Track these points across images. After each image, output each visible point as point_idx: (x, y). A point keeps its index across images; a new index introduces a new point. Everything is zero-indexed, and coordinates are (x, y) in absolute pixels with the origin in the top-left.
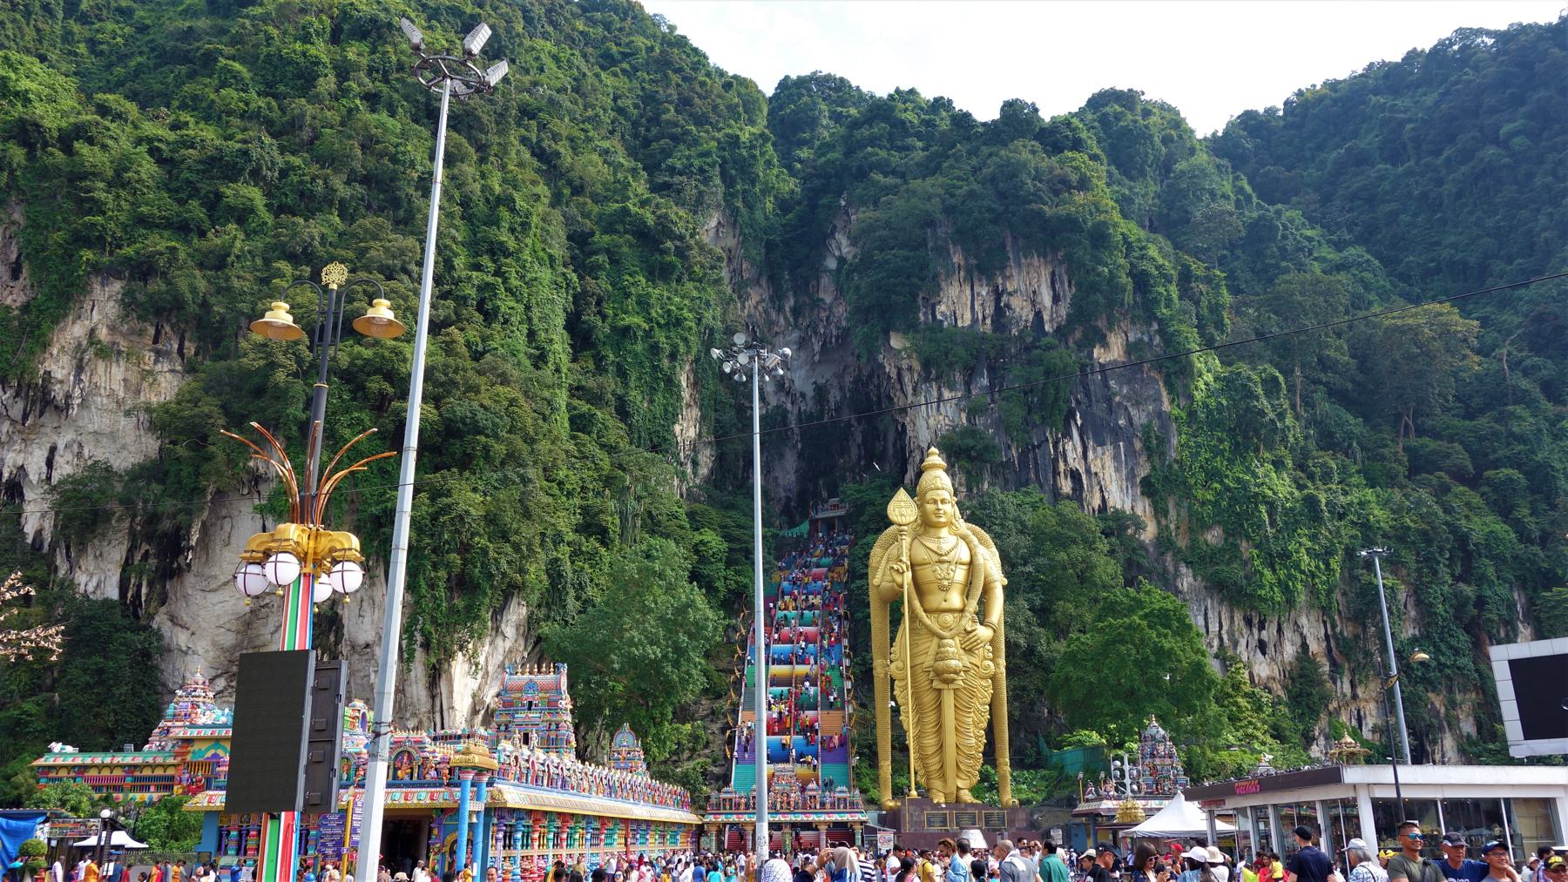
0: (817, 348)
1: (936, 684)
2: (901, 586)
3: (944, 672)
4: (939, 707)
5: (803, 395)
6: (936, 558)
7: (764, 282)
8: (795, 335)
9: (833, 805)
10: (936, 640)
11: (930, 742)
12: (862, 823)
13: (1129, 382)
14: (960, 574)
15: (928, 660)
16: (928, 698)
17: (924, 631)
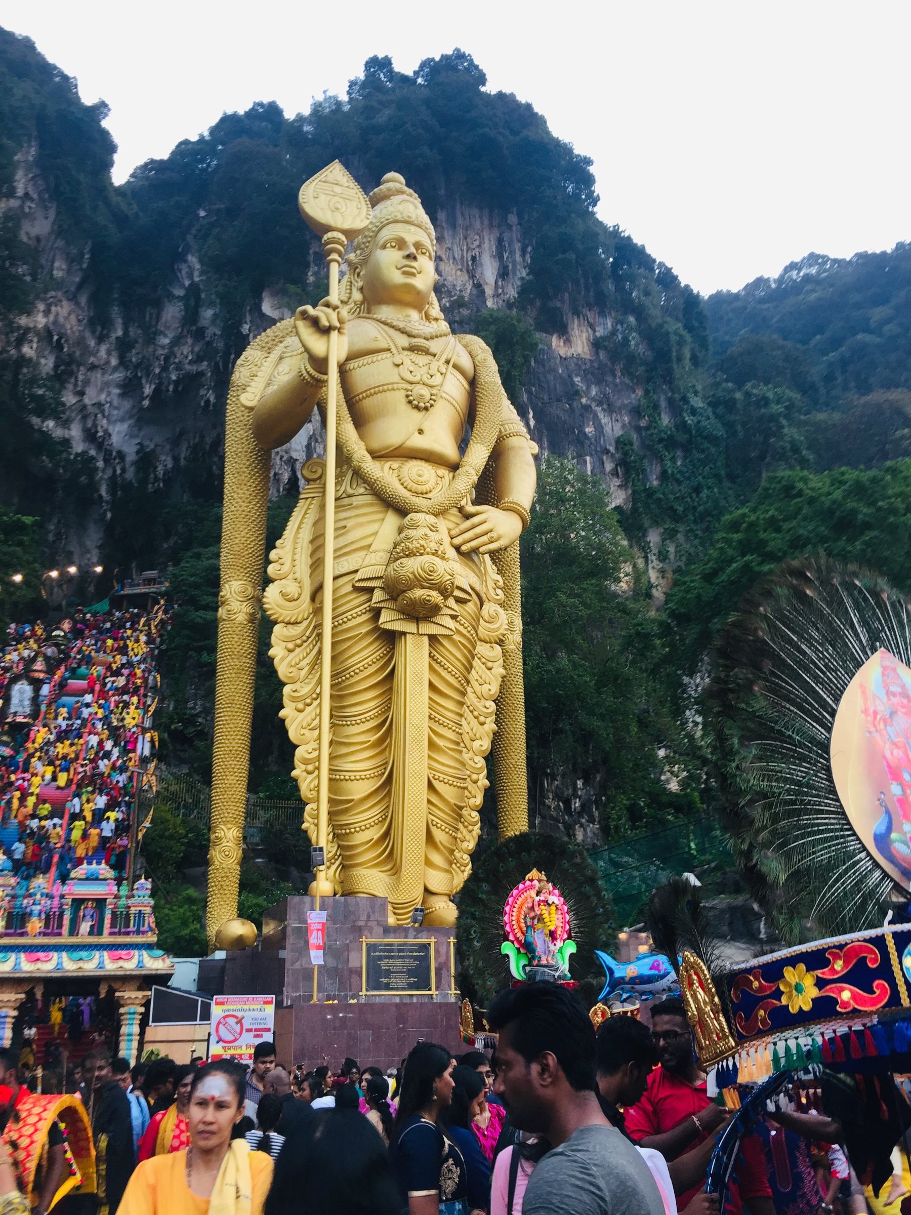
0: (148, 390)
1: (389, 620)
2: (320, 364)
3: (420, 582)
4: (388, 681)
5: (121, 455)
6: (404, 341)
7: (83, 300)
8: (119, 376)
9: (52, 922)
10: (391, 520)
11: (361, 767)
12: (147, 981)
13: (599, 382)
14: (454, 388)
15: (372, 564)
16: (365, 656)
17: (362, 498)
